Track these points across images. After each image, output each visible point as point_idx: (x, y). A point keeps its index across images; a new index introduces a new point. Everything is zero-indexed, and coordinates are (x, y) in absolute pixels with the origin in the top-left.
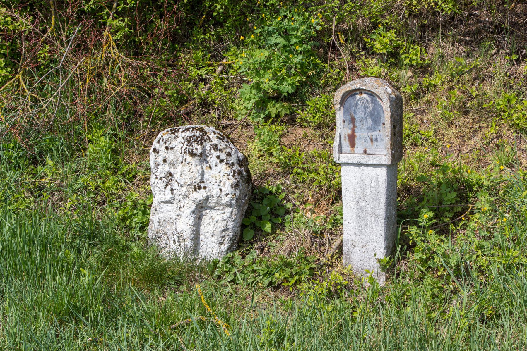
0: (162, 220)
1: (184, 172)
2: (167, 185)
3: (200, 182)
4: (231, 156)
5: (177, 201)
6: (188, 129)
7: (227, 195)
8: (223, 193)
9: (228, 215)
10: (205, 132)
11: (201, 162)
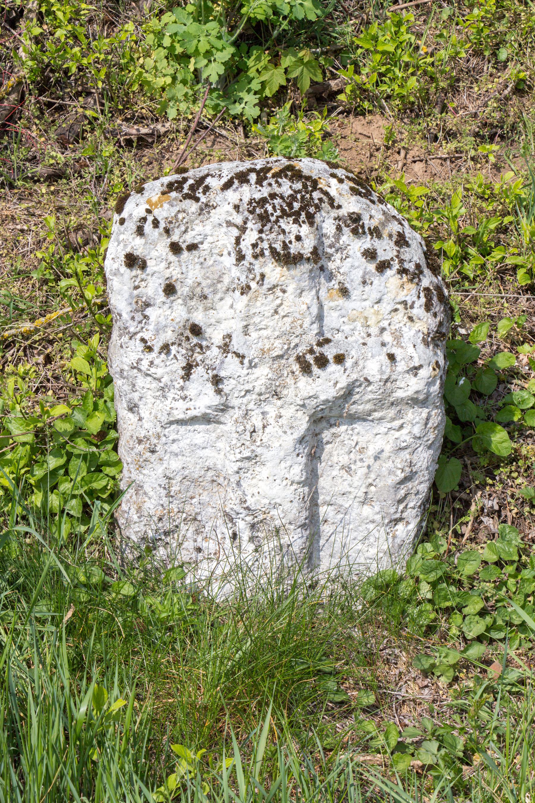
0: (179, 478)
1: (257, 319)
2: (188, 369)
3: (320, 344)
4: (408, 245)
5: (237, 413)
6: (243, 178)
7: (415, 370)
8: (401, 366)
9: (417, 430)
10: (308, 178)
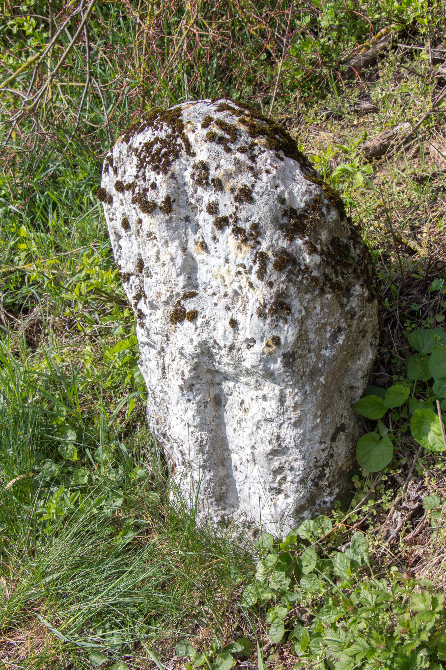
4: (251, 200)
7: (250, 343)
8: (242, 336)
11: (176, 229)
